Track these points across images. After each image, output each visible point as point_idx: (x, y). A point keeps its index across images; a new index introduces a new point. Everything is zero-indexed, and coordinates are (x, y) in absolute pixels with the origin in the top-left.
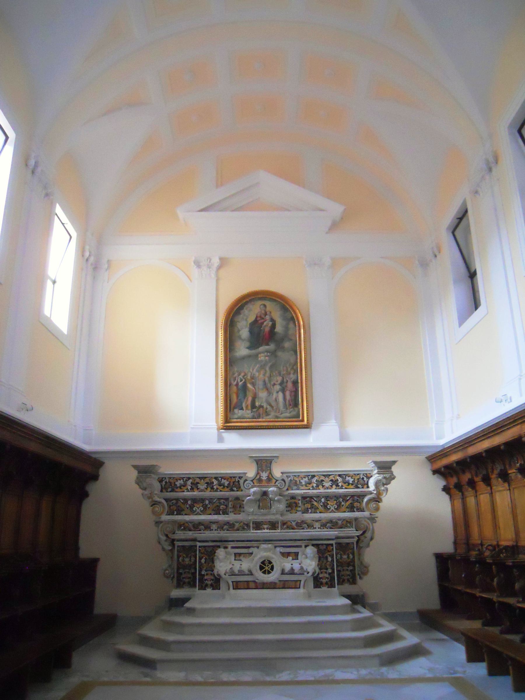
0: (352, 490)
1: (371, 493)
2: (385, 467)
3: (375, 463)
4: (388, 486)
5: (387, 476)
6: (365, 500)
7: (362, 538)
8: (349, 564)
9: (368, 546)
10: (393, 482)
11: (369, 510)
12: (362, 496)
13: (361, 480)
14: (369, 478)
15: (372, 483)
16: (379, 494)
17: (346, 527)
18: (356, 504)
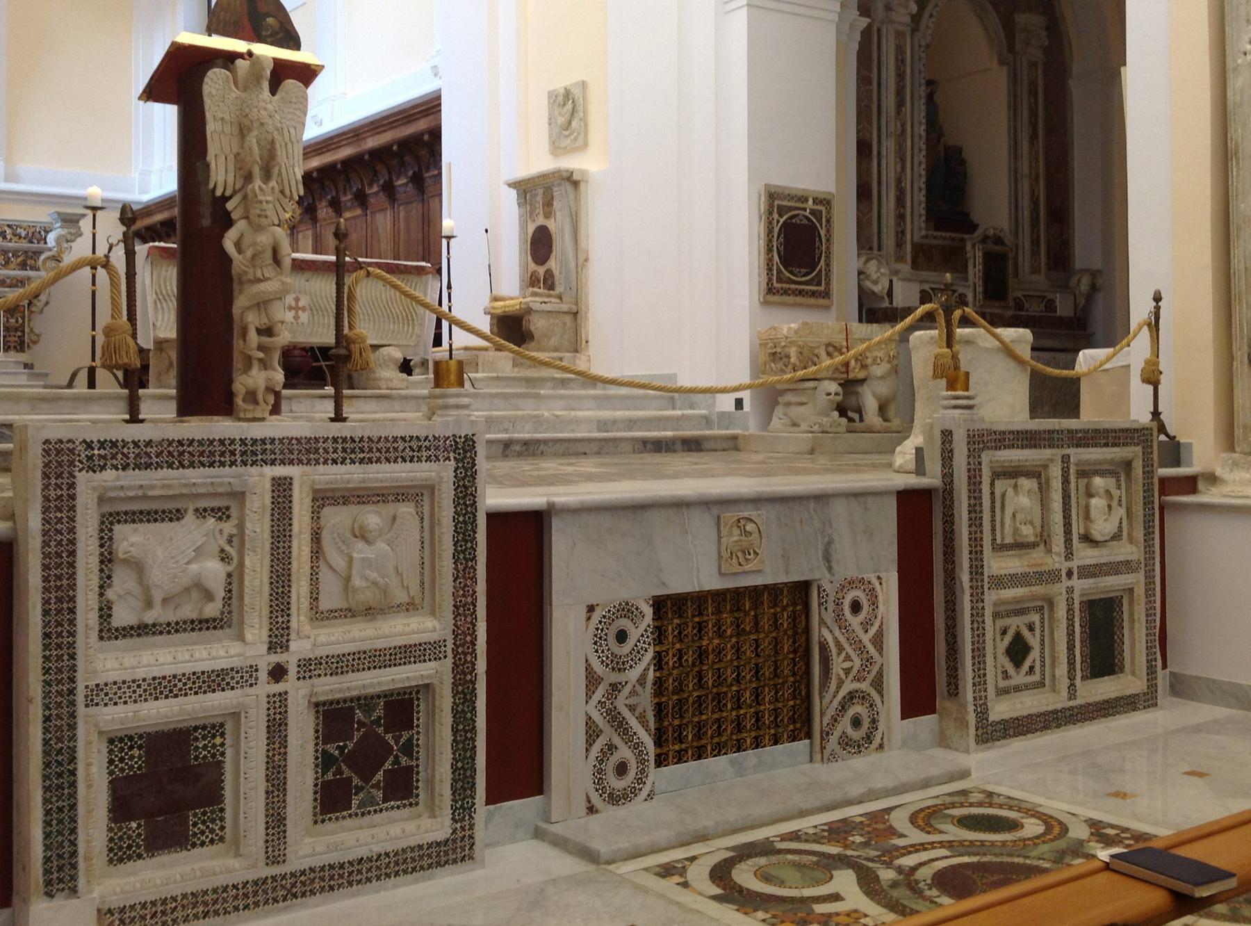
0: (24, 244)
1: (50, 250)
2: (71, 221)
3: (59, 214)
4: (73, 244)
5: (72, 231)
6: (42, 257)
7: (35, 302)
8: (16, 330)
9: (41, 312)
10: (79, 240)
11: (46, 270)
12: (38, 253)
13: (37, 235)
14: (47, 232)
15: (51, 238)
16: (60, 252)
17: (16, 286)
18: (29, 262)
